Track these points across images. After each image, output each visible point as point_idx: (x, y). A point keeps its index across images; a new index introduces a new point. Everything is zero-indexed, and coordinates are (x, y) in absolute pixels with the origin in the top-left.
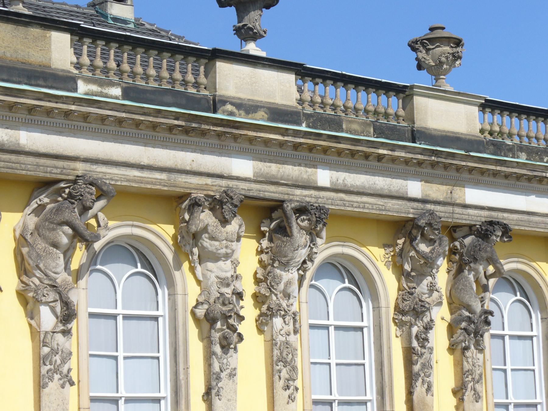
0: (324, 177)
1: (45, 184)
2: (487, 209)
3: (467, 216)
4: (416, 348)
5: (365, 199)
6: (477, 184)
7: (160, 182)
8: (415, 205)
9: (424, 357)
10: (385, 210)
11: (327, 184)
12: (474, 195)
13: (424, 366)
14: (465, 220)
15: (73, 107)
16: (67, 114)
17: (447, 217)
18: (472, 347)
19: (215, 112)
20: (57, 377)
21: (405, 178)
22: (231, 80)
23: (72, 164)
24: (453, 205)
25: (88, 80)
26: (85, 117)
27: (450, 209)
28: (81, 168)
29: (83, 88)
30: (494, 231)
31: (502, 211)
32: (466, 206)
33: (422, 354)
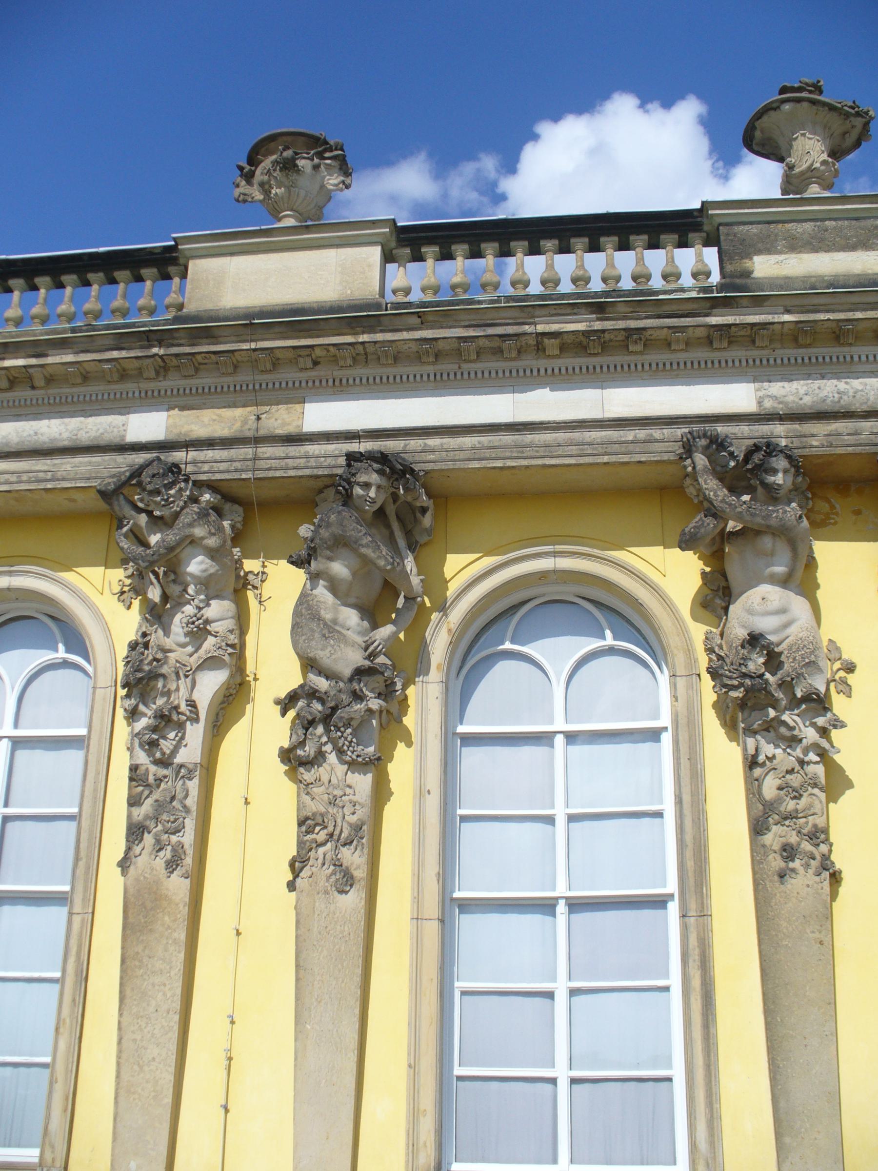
2: (366, 437)
3: (303, 461)
4: (143, 768)
6: (340, 389)
9: (163, 785)
12: (322, 415)
13: (160, 807)
14: (294, 468)
17: (236, 471)
18: (332, 758)
21: (125, 410)
24: (258, 441)
27: (247, 451)
30: (354, 475)
31: (419, 435)
33: (159, 780)
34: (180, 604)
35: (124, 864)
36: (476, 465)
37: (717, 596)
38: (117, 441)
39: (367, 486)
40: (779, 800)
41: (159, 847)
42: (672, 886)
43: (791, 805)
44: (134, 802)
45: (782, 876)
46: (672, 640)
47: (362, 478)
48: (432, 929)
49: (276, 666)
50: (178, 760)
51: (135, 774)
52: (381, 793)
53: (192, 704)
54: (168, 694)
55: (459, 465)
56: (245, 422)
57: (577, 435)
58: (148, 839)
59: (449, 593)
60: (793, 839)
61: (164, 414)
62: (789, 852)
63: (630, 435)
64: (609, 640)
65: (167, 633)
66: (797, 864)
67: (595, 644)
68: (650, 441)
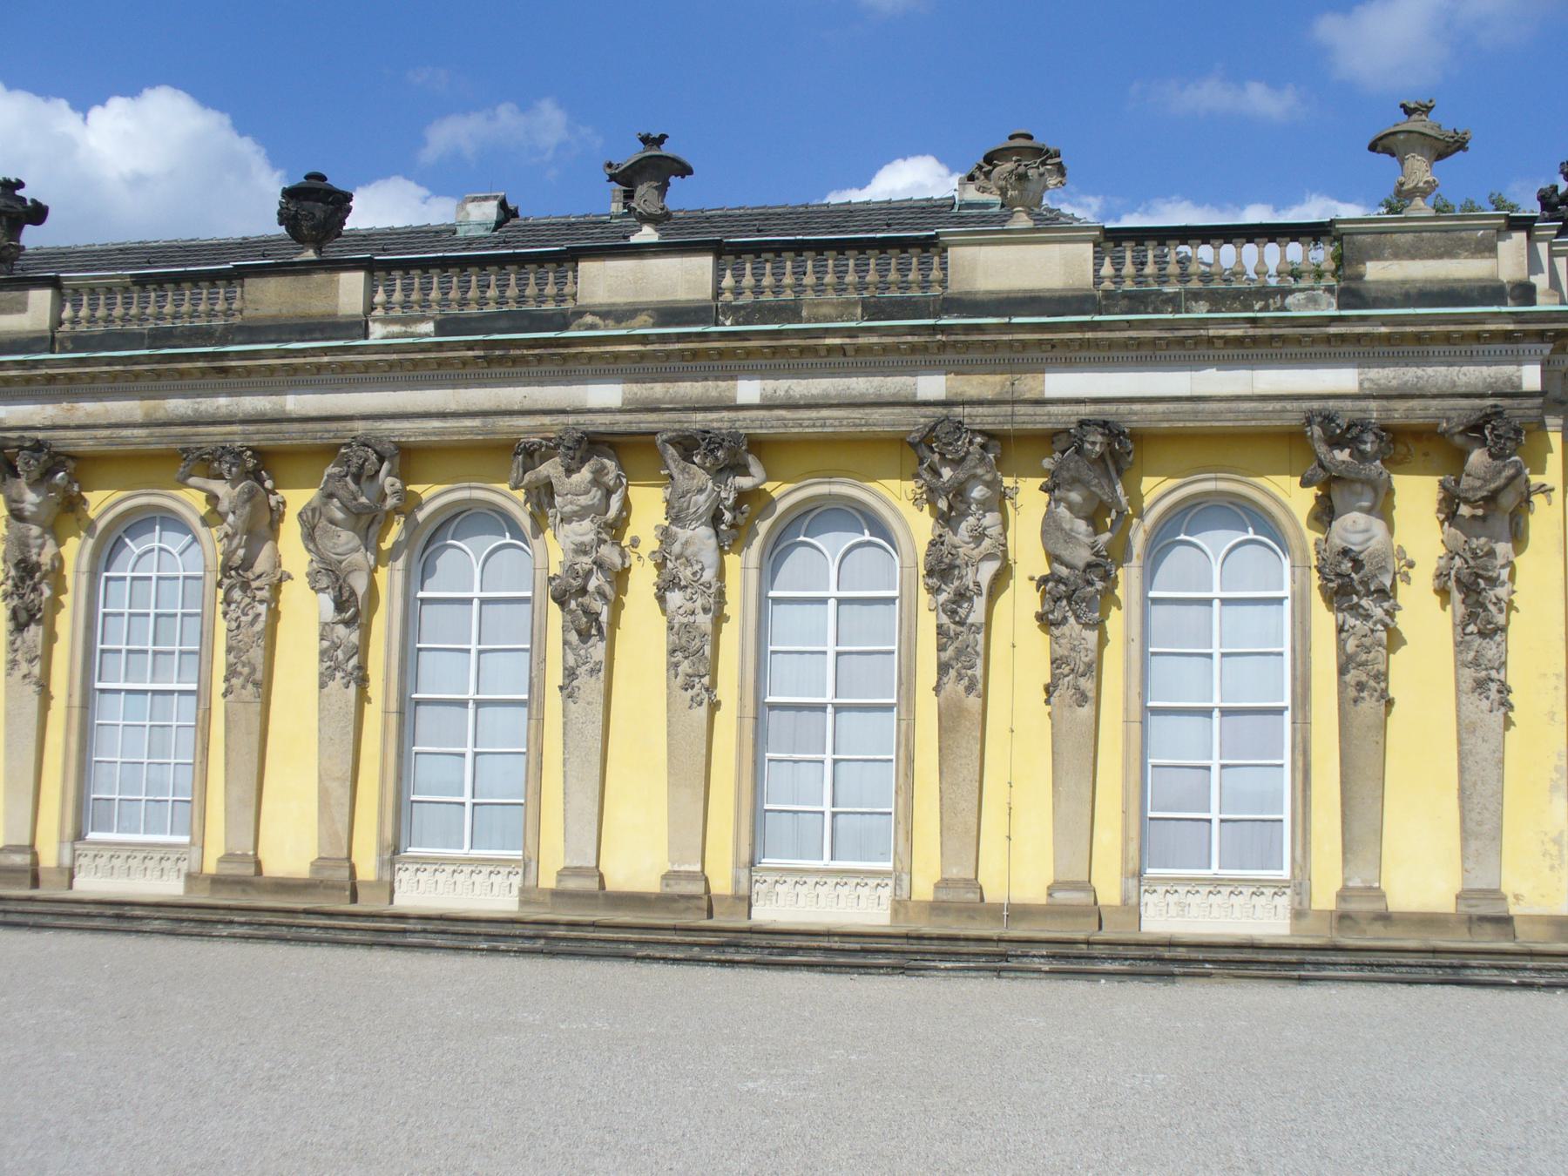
0: (748, 390)
1: (330, 452)
5: (825, 413)
6: (1070, 365)
7: (472, 430)
8: (930, 411)
10: (866, 425)
11: (756, 400)
12: (1060, 384)
13: (959, 652)
15: (326, 359)
16: (319, 368)
18: (1072, 620)
19: (366, 337)
20: (339, 675)
21: (914, 373)
22: (601, 281)
23: (349, 425)
24: (1014, 402)
25: (386, 321)
26: (344, 367)
27: (1008, 409)
28: (360, 427)
29: (378, 333)
32: (1041, 402)
33: (957, 635)
34: (963, 515)
35: (937, 689)
36: (1165, 425)
37: (1325, 514)
38: (910, 399)
39: (1094, 443)
40: (1356, 654)
41: (960, 677)
42: (1287, 702)
43: (1364, 657)
44: (941, 648)
45: (1355, 701)
46: (1293, 542)
47: (1092, 439)
48: (1136, 727)
49: (1030, 559)
50: (969, 621)
51: (941, 631)
52: (1103, 641)
53: (977, 584)
54: (961, 578)
55: (1153, 425)
56: (1003, 386)
57: (1234, 405)
58: (952, 673)
59: (1145, 505)
60: (1364, 678)
61: (943, 378)
62: (1361, 686)
63: (1270, 406)
64: (1251, 535)
65: (955, 533)
66: (1365, 694)
67: (1242, 537)
68: (1284, 411)
